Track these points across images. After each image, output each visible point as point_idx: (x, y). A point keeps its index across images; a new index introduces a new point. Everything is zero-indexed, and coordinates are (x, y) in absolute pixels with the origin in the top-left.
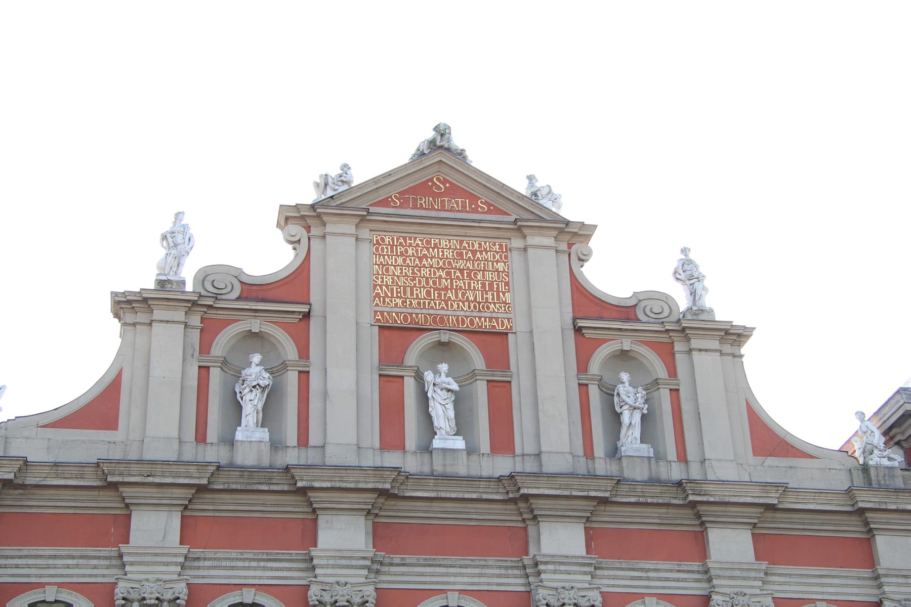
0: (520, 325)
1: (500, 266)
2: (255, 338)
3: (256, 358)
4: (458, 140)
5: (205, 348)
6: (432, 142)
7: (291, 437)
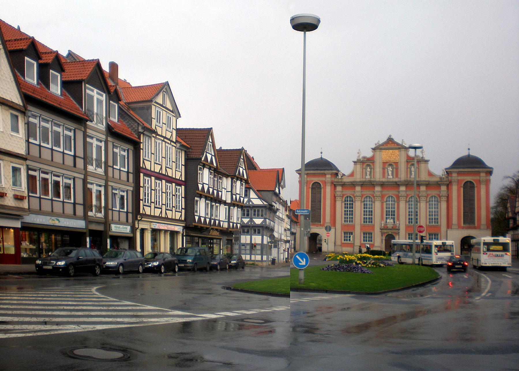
0: (400, 161)
1: (398, 153)
2: (368, 165)
3: (368, 168)
4: (393, 137)
5: (363, 166)
6: (389, 138)
7: (372, 177)
